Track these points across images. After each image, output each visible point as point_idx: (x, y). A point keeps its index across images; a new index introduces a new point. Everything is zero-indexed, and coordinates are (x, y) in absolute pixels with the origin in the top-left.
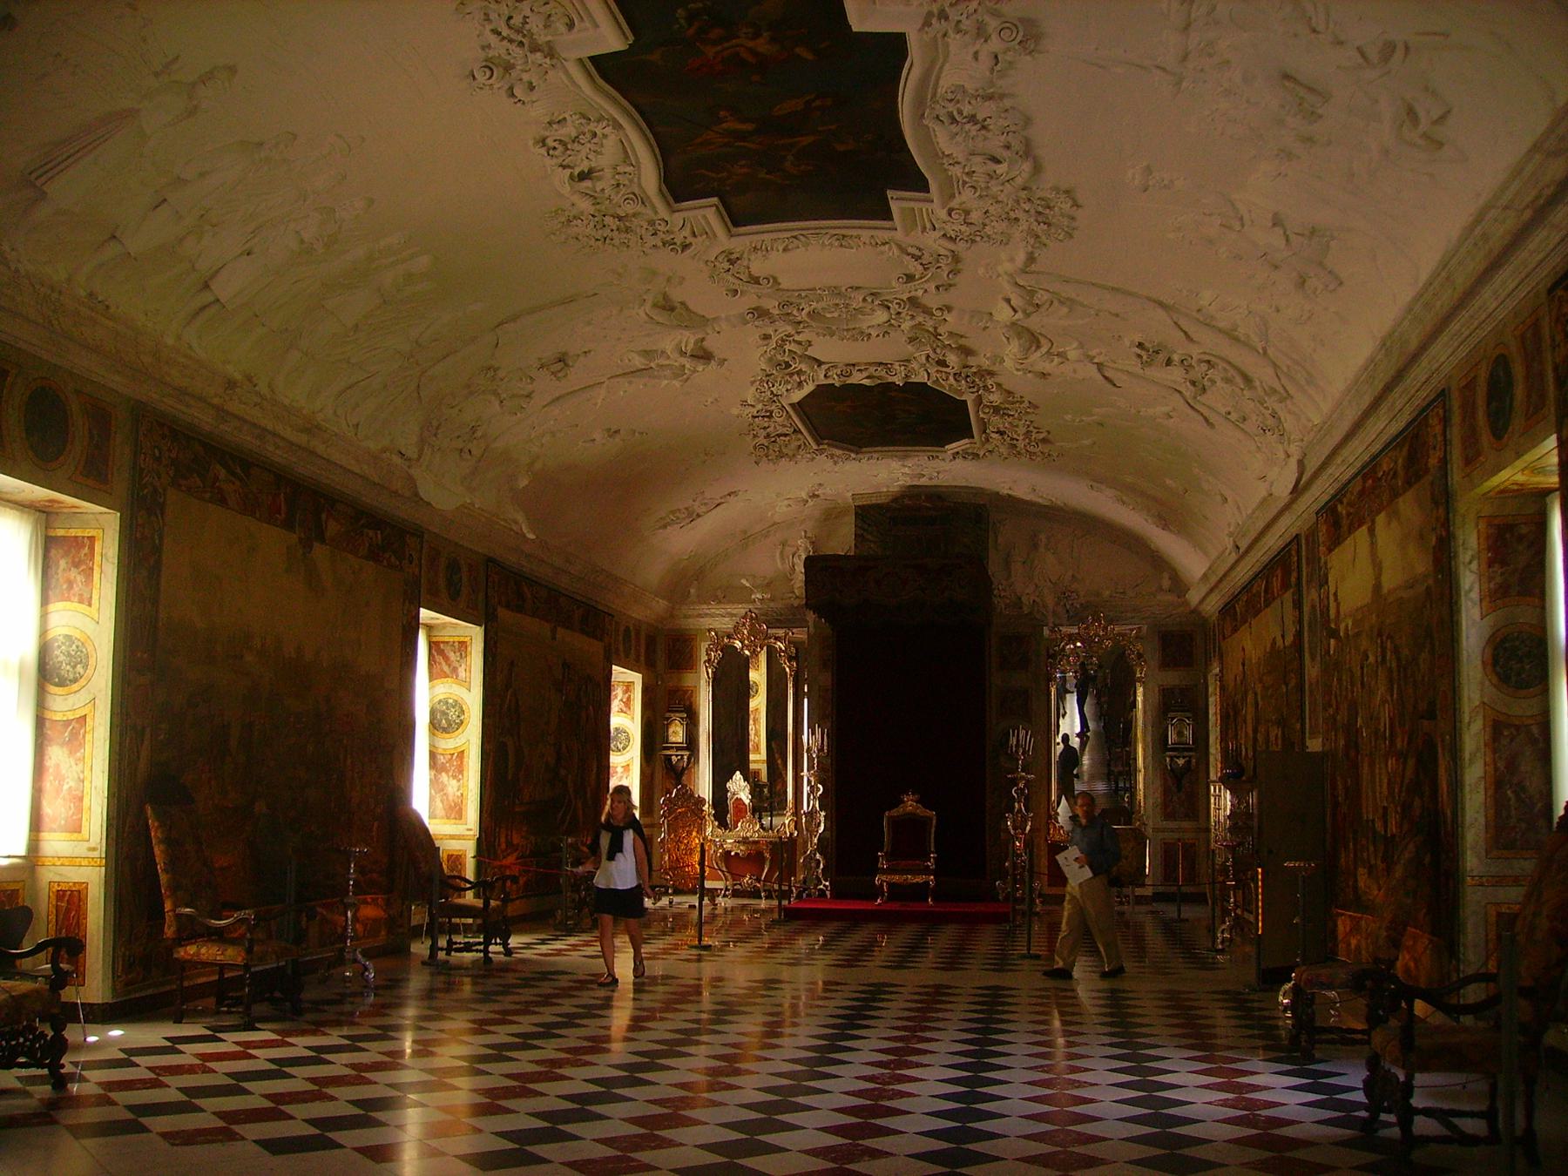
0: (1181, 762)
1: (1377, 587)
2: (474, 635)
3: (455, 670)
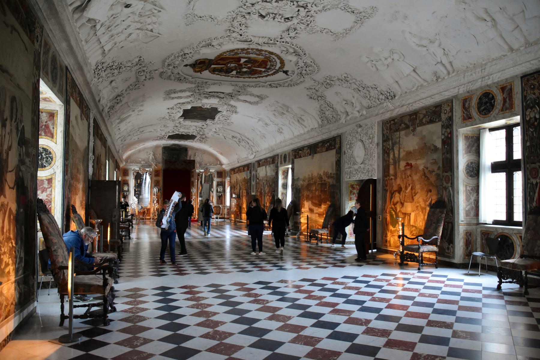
1: (266, 175)
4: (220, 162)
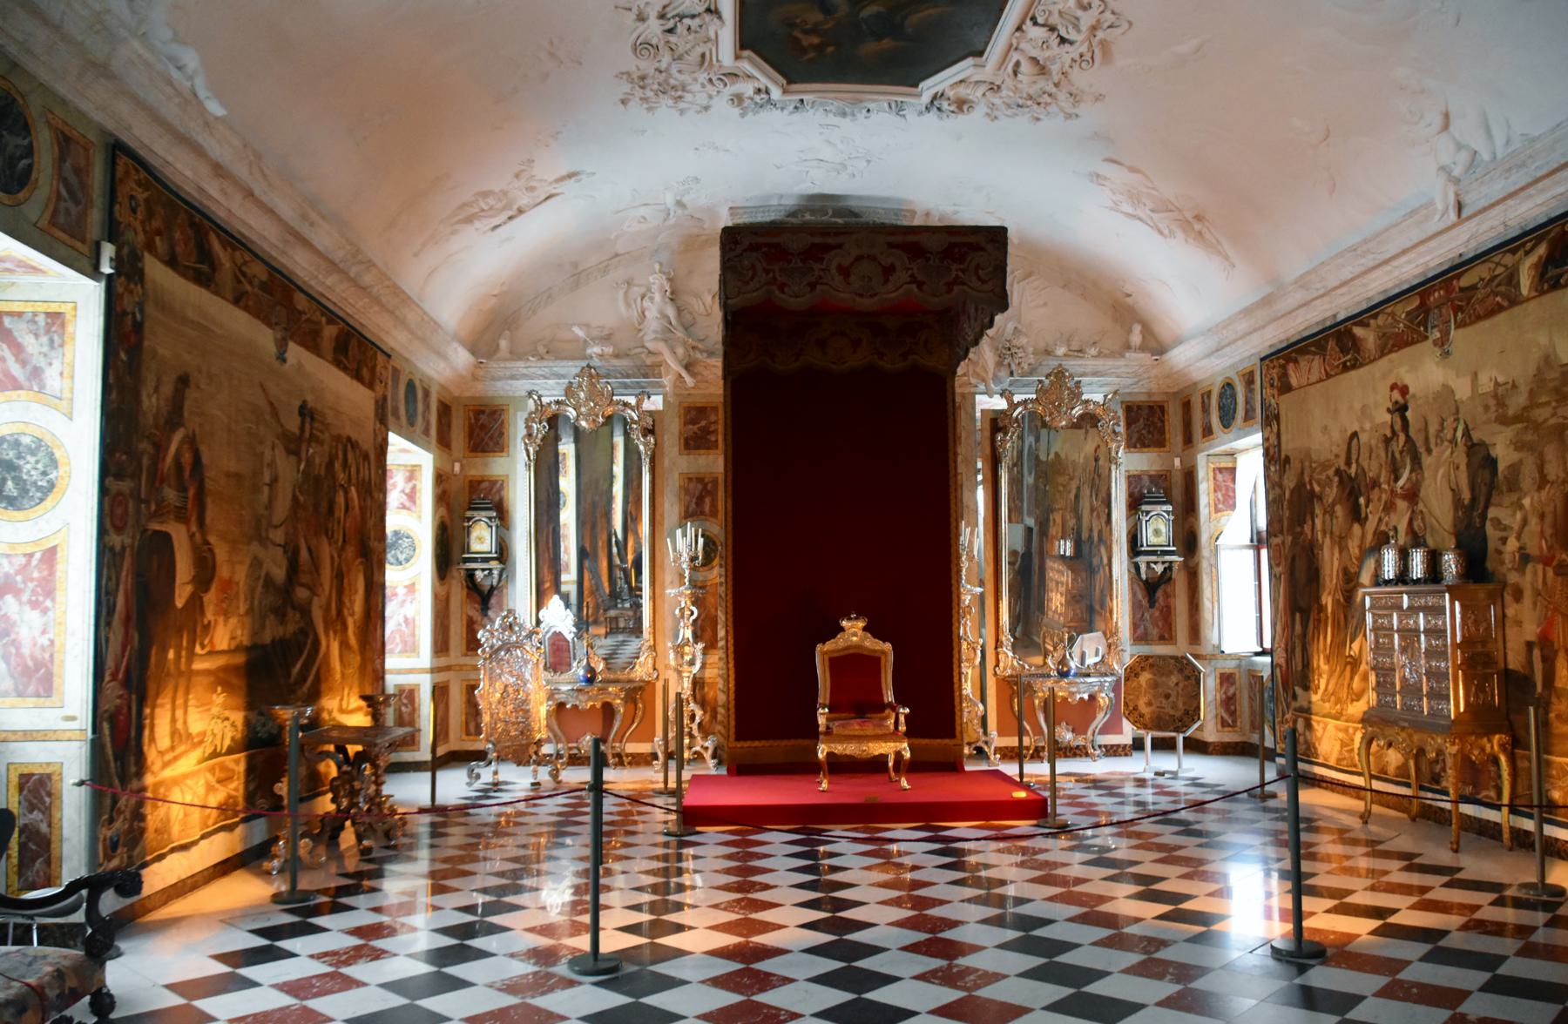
0: (1159, 569)
2: (82, 299)
3: (36, 373)
4: (1147, 330)
